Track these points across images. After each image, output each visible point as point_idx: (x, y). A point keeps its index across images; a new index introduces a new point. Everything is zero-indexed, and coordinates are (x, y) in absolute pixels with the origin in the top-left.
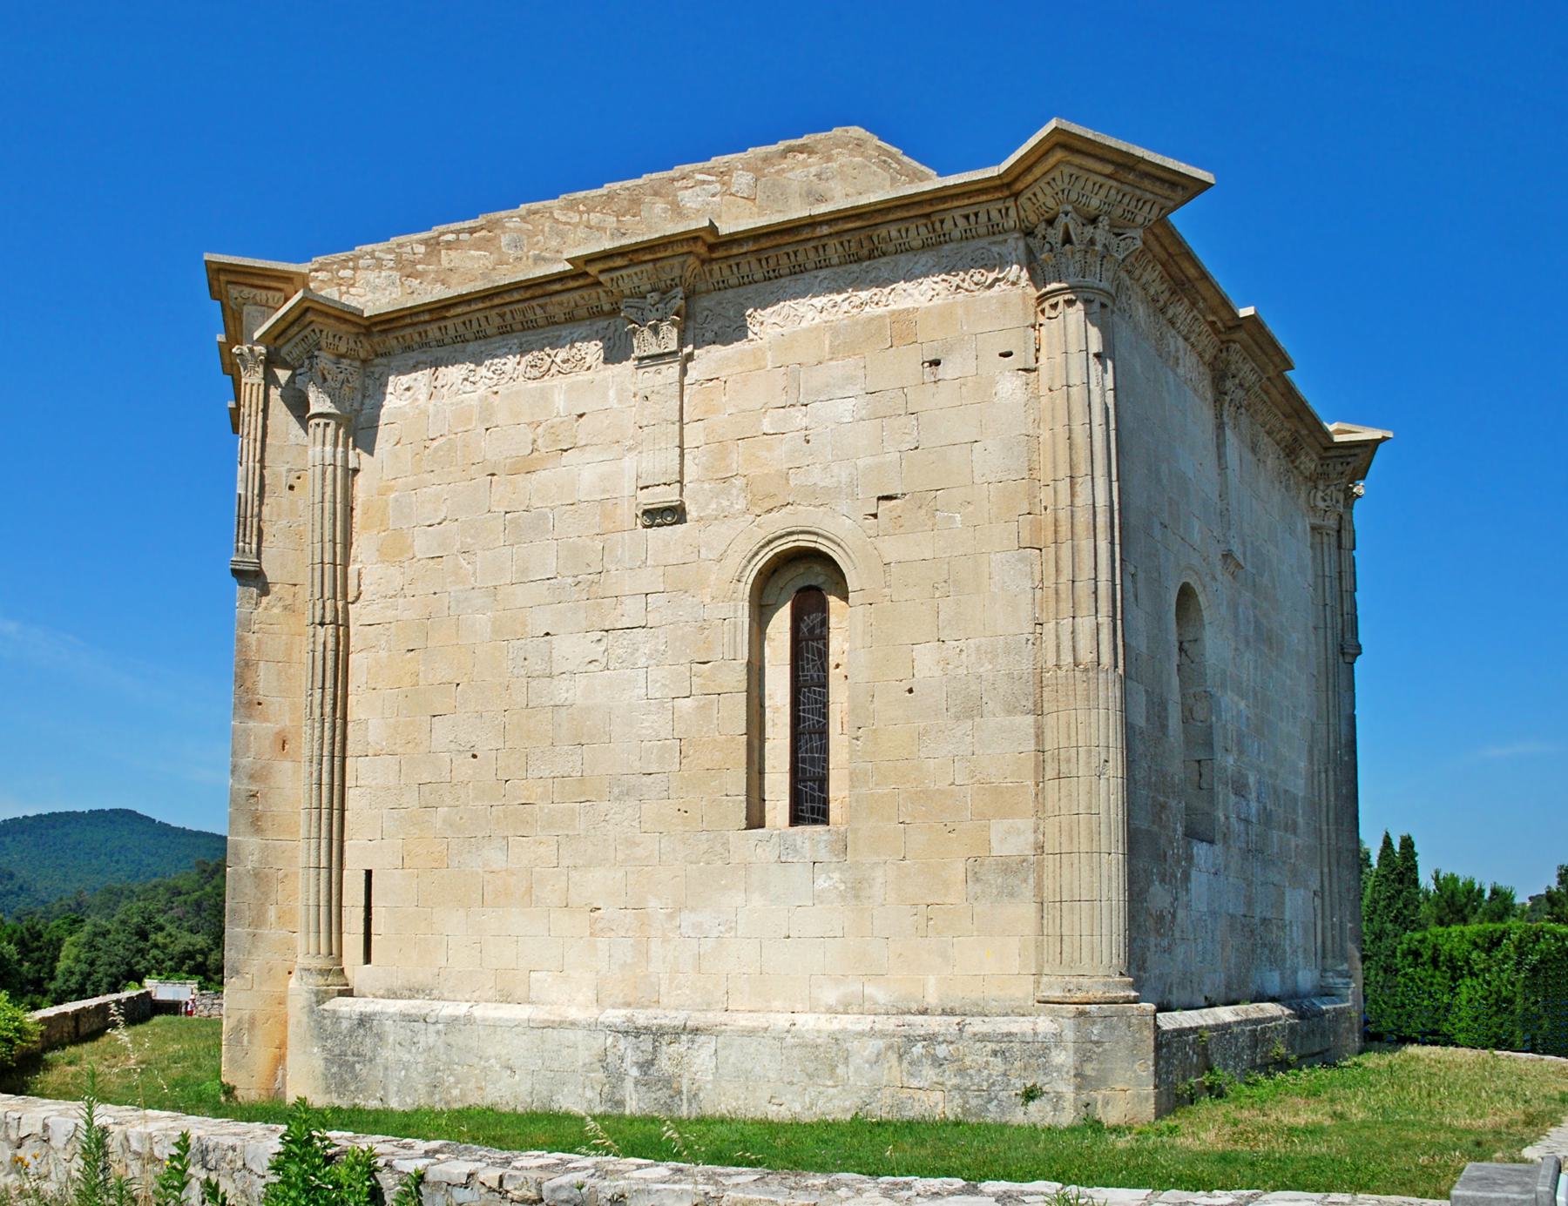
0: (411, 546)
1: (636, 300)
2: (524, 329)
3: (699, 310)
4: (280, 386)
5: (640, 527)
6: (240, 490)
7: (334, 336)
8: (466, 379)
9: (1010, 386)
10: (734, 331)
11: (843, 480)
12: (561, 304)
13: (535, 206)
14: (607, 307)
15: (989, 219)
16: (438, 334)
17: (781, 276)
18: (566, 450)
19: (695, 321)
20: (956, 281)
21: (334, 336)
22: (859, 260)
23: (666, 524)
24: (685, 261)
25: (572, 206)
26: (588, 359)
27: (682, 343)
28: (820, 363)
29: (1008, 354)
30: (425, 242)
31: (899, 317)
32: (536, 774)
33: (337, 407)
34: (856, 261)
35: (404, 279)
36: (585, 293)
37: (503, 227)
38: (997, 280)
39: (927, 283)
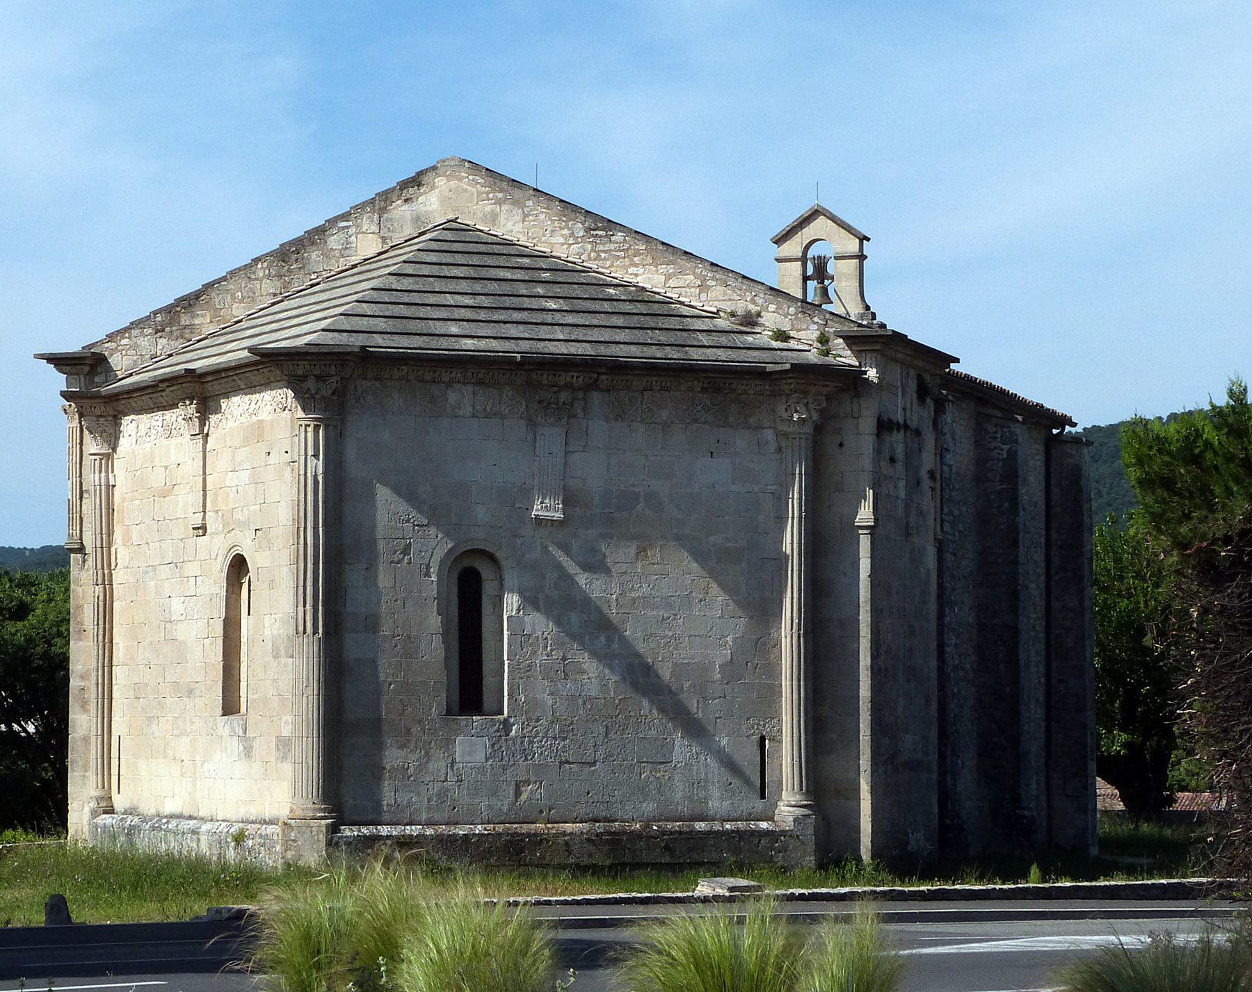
6: (70, 497)
7: (91, 407)
21: (91, 407)
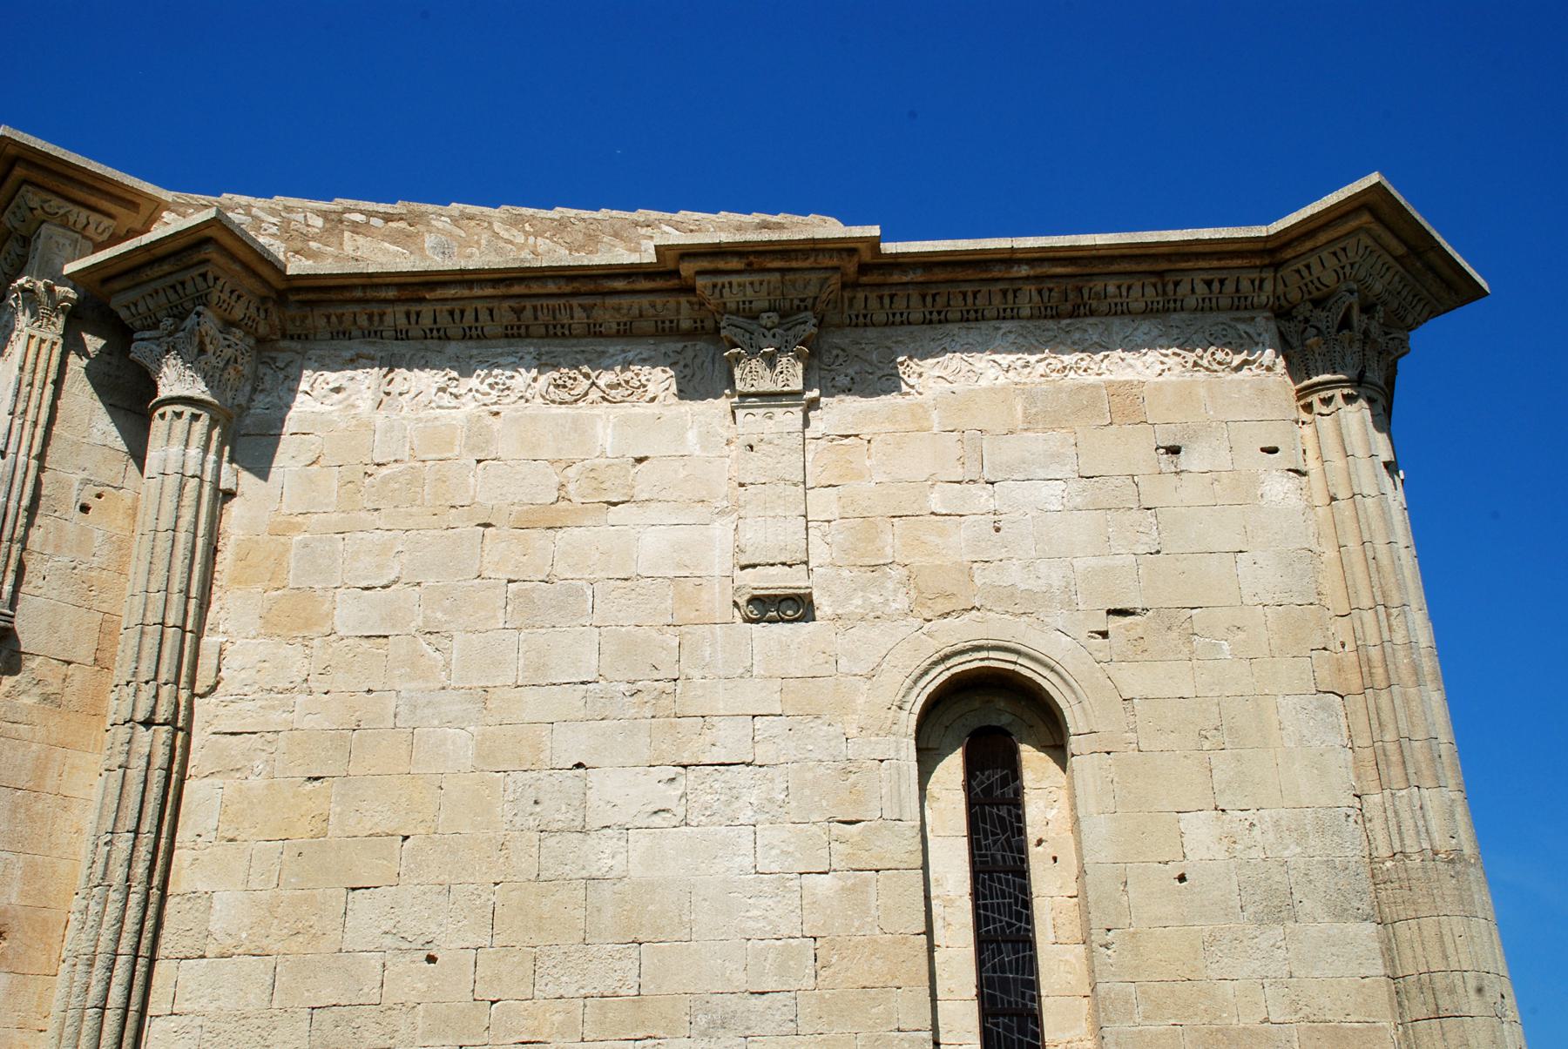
0: (329, 616)
1: (741, 319)
2: (547, 336)
3: (826, 347)
4: (87, 355)
5: (739, 620)
7: (232, 292)
8: (443, 390)
9: (1278, 488)
10: (888, 382)
11: (1056, 584)
12: (618, 309)
13: (471, 209)
14: (685, 324)
15: (1237, 290)
16: (402, 322)
17: (947, 321)
18: (615, 504)
19: (820, 360)
20: (1191, 357)
22: (1058, 316)
23: (783, 620)
24: (827, 279)
25: (516, 222)
26: (650, 387)
27: (807, 386)
28: (1012, 433)
29: (1273, 451)
30: (324, 215)
31: (1116, 390)
32: (552, 990)
33: (213, 396)
34: (1052, 317)
35: (290, 254)
36: (659, 300)
37: (428, 224)
38: (1245, 362)
39: (1152, 356)
